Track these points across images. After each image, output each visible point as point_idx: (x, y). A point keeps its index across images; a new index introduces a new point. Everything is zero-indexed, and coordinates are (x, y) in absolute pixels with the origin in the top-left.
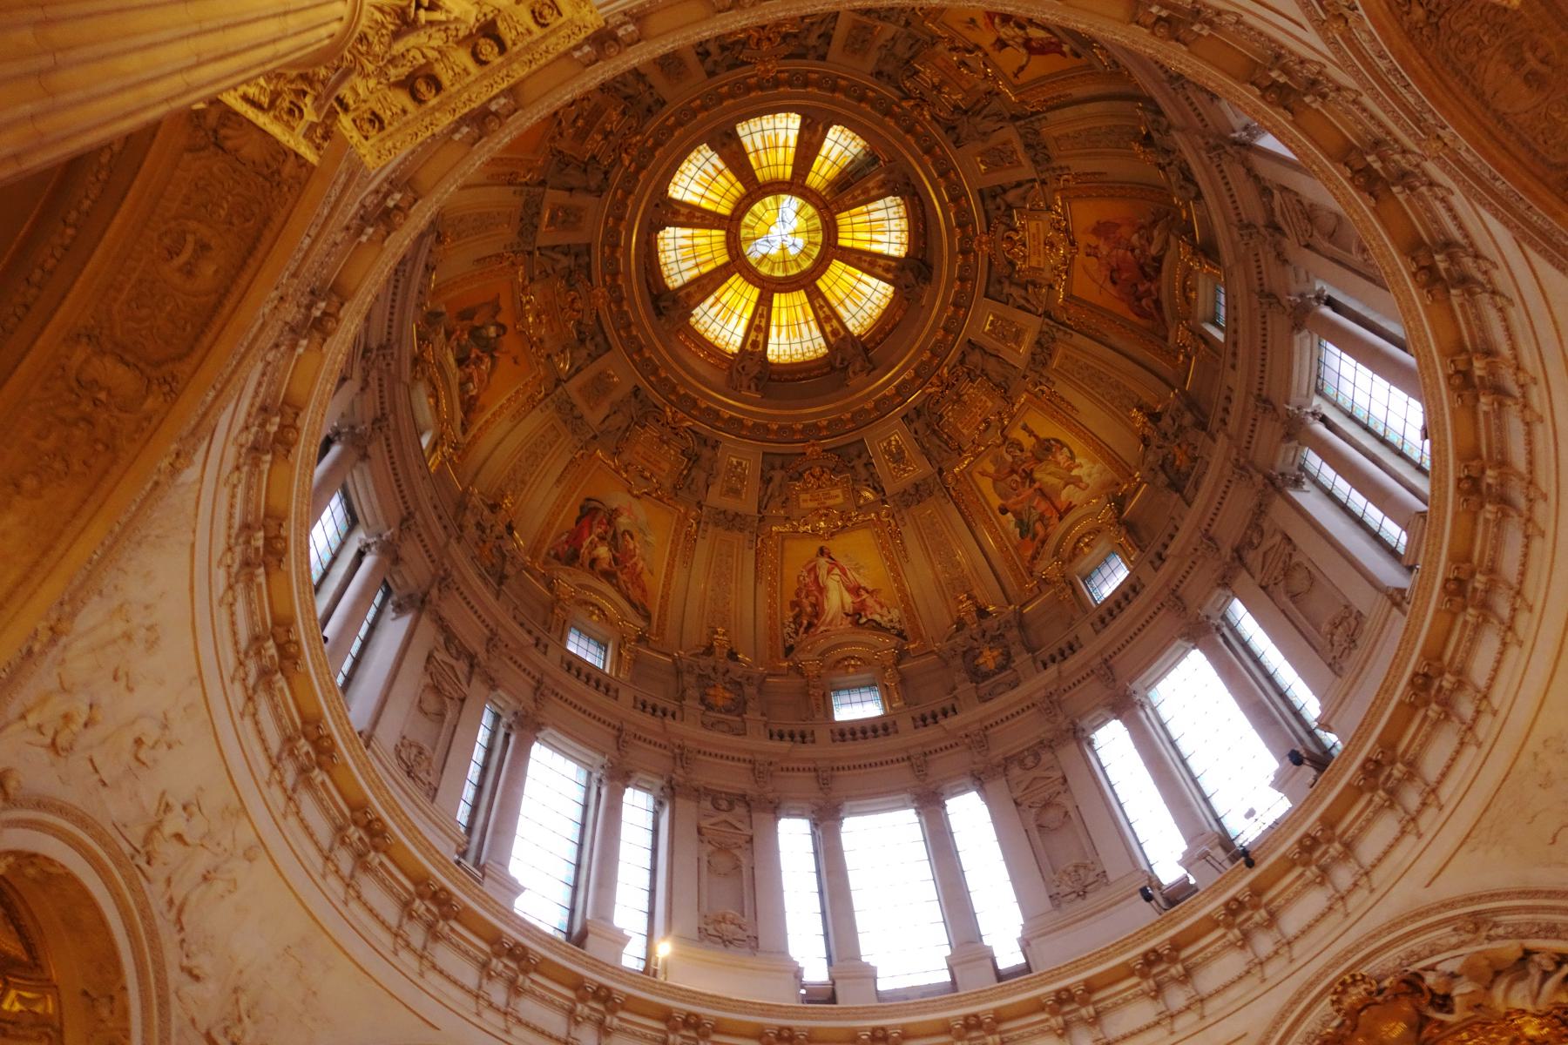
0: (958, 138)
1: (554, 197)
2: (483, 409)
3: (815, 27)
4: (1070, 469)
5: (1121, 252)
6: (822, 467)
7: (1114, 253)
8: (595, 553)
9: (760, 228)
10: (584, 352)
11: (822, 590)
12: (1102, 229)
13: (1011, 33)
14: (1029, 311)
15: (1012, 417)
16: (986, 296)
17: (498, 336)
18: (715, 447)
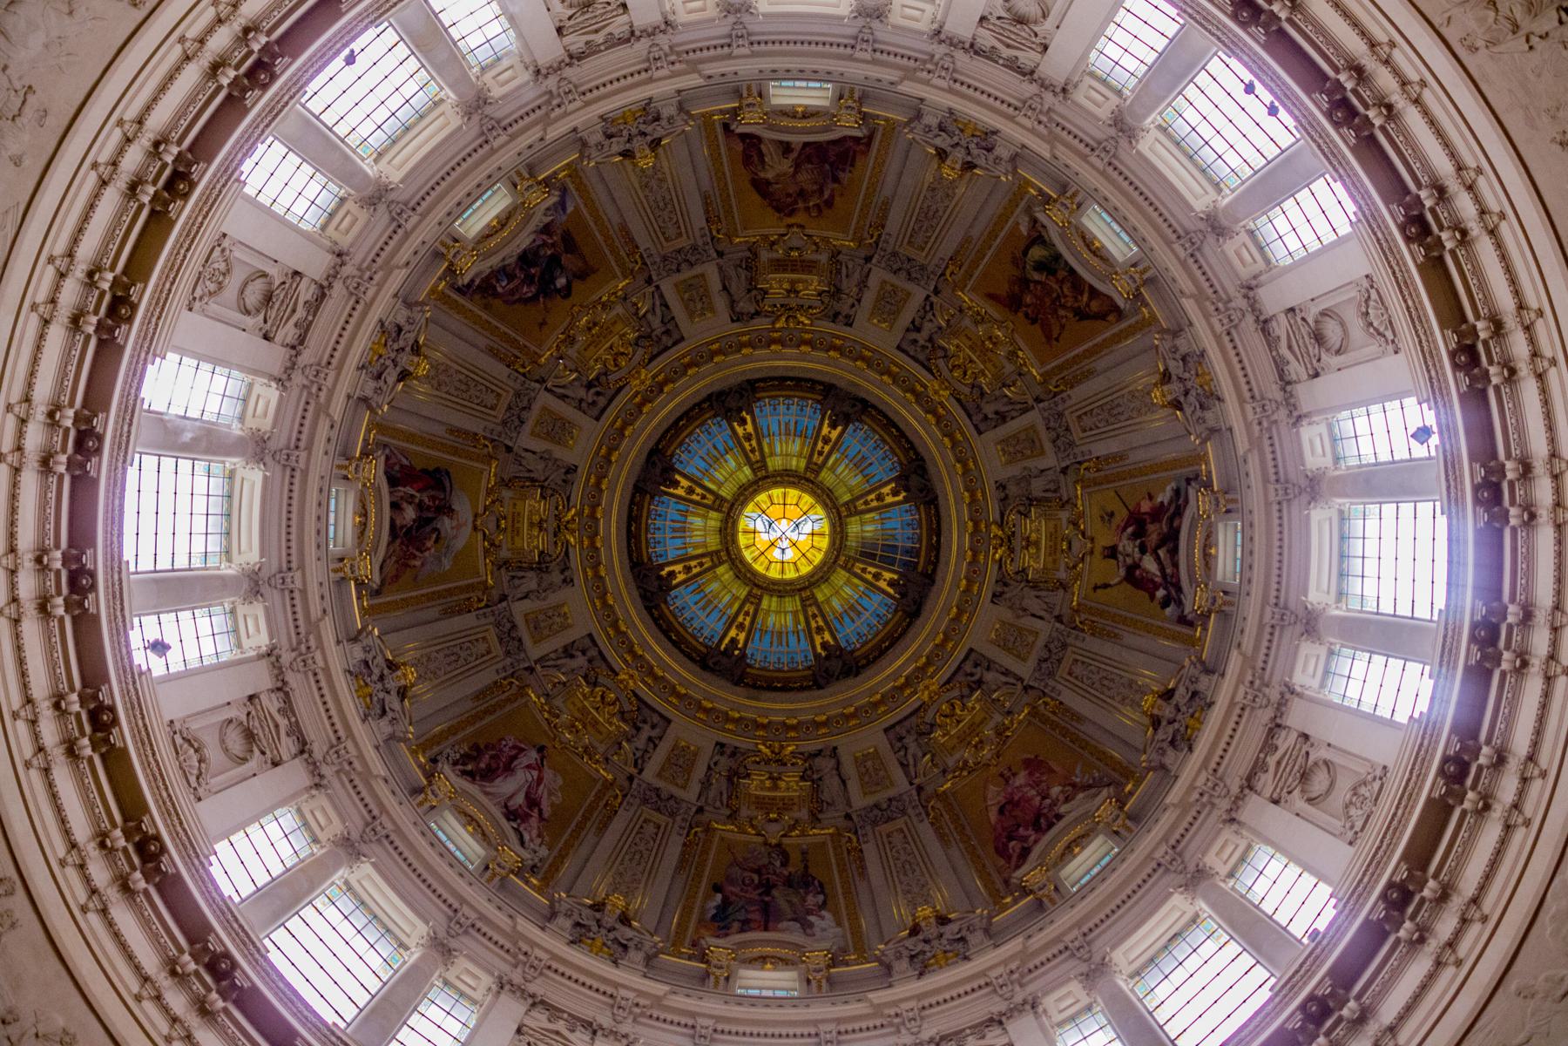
0: (1002, 593)
2: (486, 307)
3: (1005, 400)
4: (810, 912)
5: (1033, 792)
6: (617, 699)
7: (1025, 790)
8: (405, 505)
9: (776, 511)
10: (582, 393)
11: (509, 769)
13: (1129, 550)
14: (907, 774)
15: (803, 834)
17: (558, 291)
18: (568, 581)
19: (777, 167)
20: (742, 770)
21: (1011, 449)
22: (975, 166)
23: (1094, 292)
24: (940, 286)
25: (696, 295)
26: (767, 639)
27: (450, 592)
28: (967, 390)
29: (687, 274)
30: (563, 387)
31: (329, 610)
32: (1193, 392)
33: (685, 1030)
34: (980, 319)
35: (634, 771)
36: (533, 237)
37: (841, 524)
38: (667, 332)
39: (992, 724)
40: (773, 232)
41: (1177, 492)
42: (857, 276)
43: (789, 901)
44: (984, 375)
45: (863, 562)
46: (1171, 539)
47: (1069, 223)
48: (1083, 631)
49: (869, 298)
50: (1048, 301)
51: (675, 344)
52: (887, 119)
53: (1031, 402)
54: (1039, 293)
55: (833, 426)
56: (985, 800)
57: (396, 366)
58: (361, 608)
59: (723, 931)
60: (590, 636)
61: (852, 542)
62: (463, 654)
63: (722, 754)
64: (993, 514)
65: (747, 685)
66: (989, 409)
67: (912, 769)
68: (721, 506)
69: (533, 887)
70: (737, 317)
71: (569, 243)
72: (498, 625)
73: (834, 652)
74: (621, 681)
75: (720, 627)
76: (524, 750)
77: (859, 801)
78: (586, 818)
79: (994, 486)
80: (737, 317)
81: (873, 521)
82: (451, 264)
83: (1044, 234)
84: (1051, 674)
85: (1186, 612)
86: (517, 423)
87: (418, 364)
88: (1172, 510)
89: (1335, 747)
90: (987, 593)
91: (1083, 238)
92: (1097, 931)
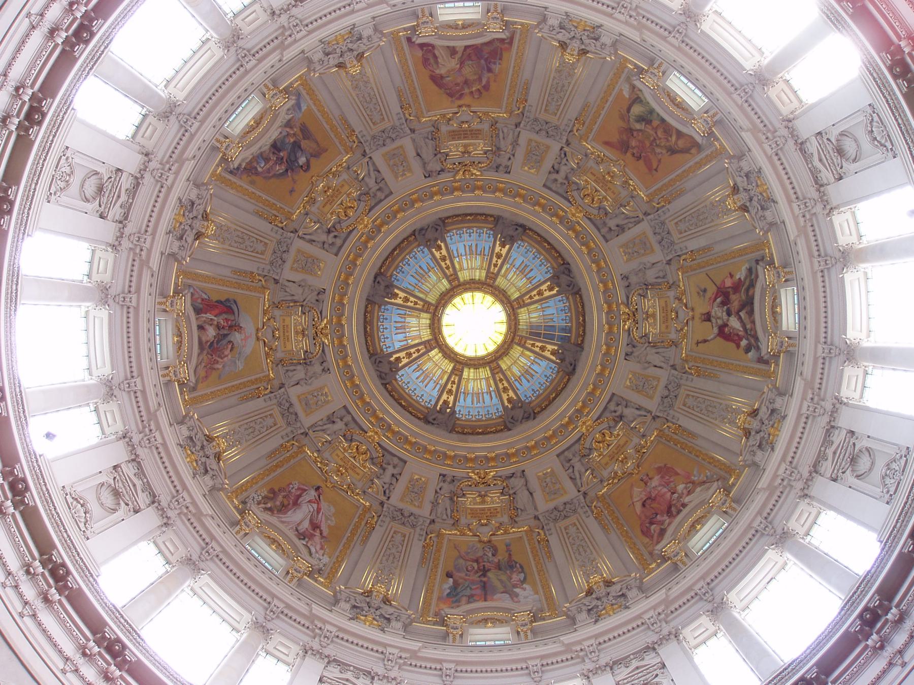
0: (632, 353)
1: (407, 143)
2: (252, 183)
3: (623, 216)
4: (515, 586)
5: (665, 490)
6: (368, 449)
7: (659, 488)
10: (323, 237)
11: (296, 504)
12: (665, 471)
13: (720, 315)
14: (575, 485)
15: (506, 532)
16: (558, 456)
18: (326, 370)
19: (447, 65)
20: (459, 492)
21: (630, 251)
22: (588, 52)
23: (680, 134)
24: (570, 140)
25: (398, 160)
26: (469, 399)
27: (244, 385)
28: (595, 212)
29: (391, 146)
30: (309, 234)
31: (162, 403)
32: (755, 199)
33: (435, 672)
34: (600, 161)
35: (384, 499)
36: (280, 130)
37: (514, 314)
38: (380, 189)
39: (632, 445)
40: (449, 111)
41: (750, 270)
42: (511, 136)
43: (500, 580)
44: (607, 199)
45: (531, 339)
46: (748, 304)
47: (658, 86)
48: (691, 374)
49: (520, 153)
50: (648, 144)
51: (386, 197)
52: (522, 24)
53: (641, 216)
54: (640, 138)
55: (503, 245)
56: (631, 497)
57: (192, 229)
58: (184, 400)
59: (457, 604)
60: (345, 407)
61: (522, 326)
62: (257, 427)
63: (444, 481)
64: (621, 296)
65: (458, 432)
66: (612, 223)
67: (578, 481)
68: (428, 308)
69: (321, 584)
70: (428, 175)
71: (305, 132)
72: (280, 405)
73: (516, 404)
74: (370, 437)
75: (435, 393)
76: (305, 490)
77: (543, 505)
78: (353, 534)
79: (620, 278)
80: (428, 175)
81: (536, 310)
82: (225, 154)
83: (641, 96)
84: (671, 406)
85: (762, 355)
86: (280, 262)
87: (208, 227)
88: (747, 283)
89: (873, 438)
90: (621, 354)
91: (669, 95)
92: (716, 581)
